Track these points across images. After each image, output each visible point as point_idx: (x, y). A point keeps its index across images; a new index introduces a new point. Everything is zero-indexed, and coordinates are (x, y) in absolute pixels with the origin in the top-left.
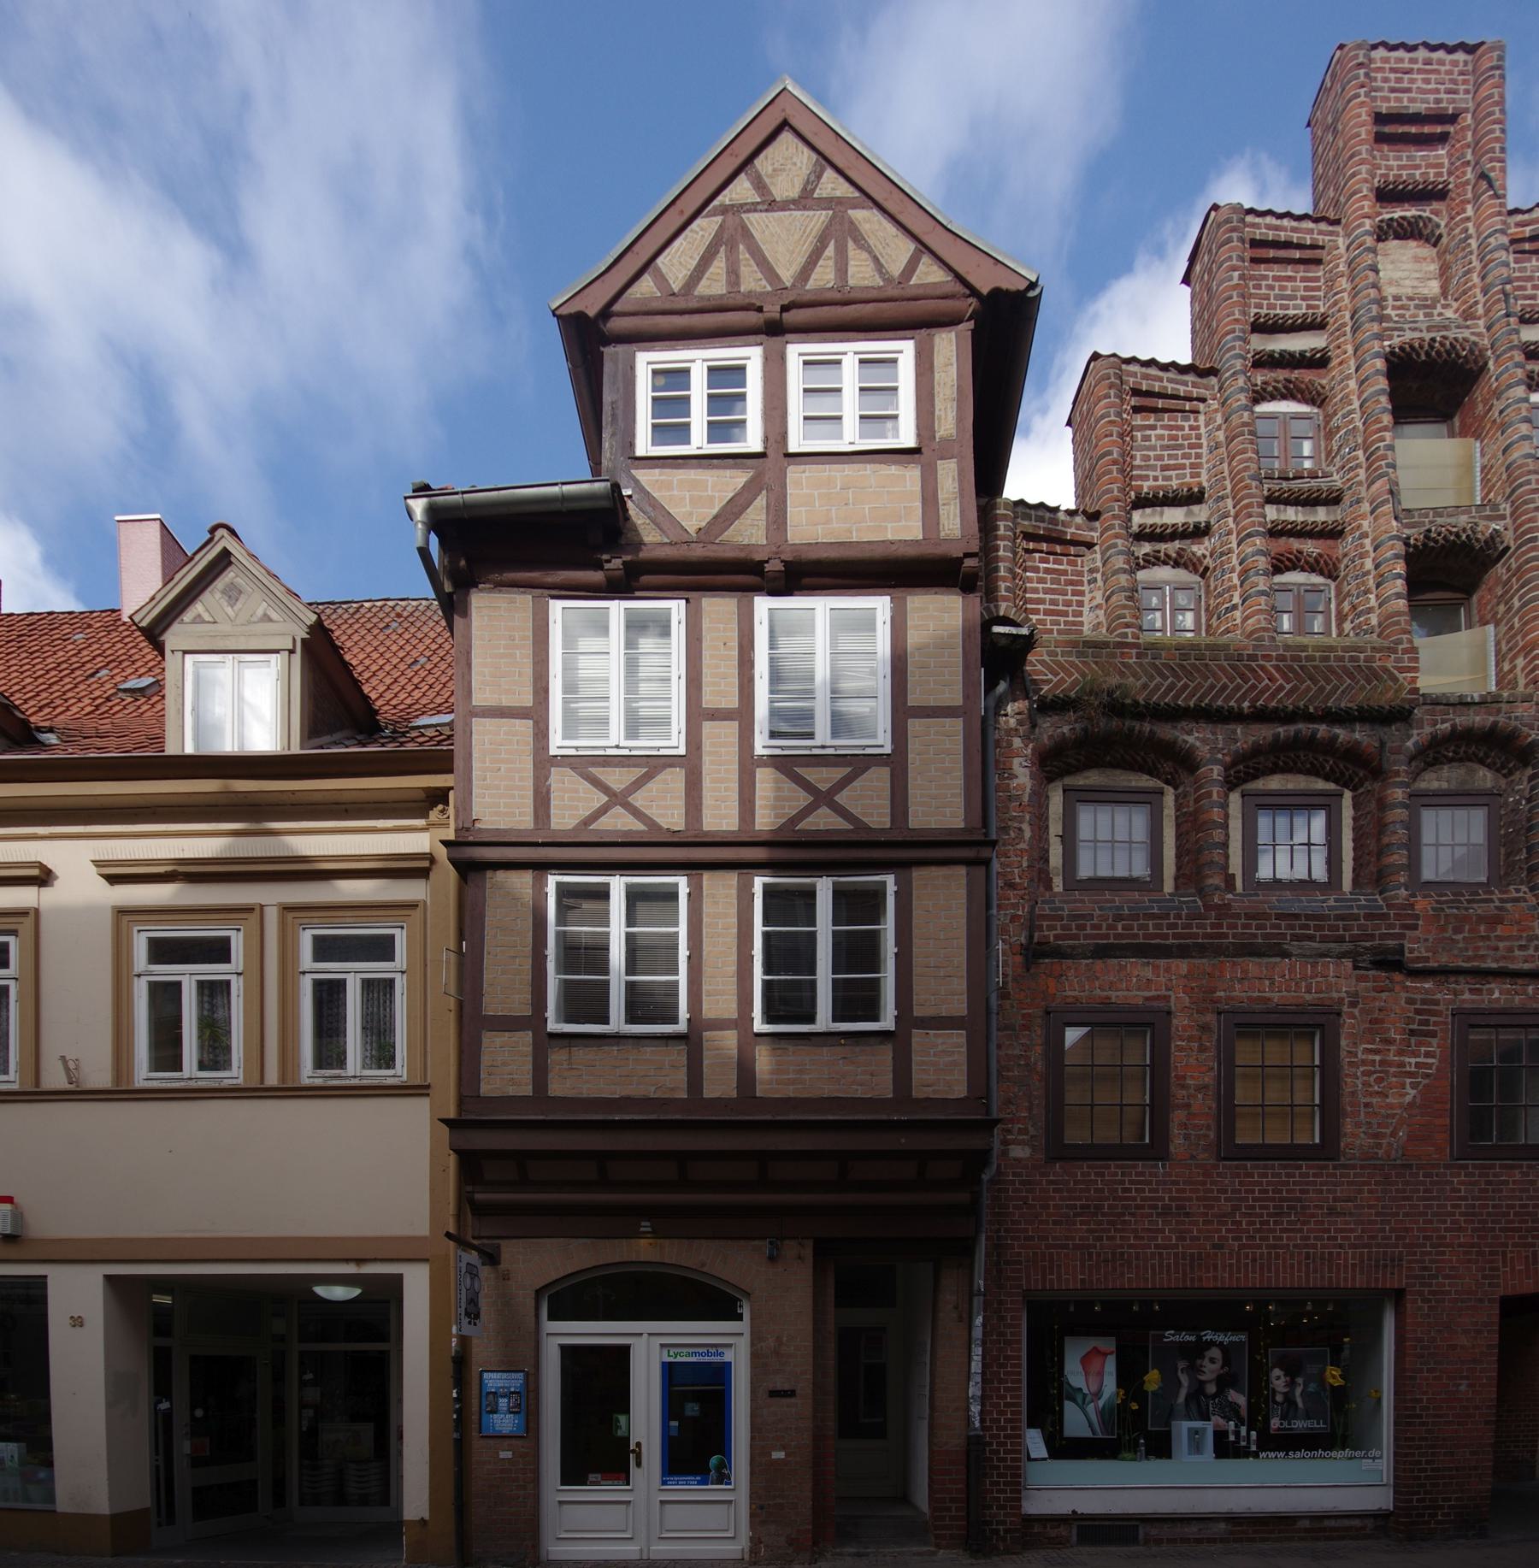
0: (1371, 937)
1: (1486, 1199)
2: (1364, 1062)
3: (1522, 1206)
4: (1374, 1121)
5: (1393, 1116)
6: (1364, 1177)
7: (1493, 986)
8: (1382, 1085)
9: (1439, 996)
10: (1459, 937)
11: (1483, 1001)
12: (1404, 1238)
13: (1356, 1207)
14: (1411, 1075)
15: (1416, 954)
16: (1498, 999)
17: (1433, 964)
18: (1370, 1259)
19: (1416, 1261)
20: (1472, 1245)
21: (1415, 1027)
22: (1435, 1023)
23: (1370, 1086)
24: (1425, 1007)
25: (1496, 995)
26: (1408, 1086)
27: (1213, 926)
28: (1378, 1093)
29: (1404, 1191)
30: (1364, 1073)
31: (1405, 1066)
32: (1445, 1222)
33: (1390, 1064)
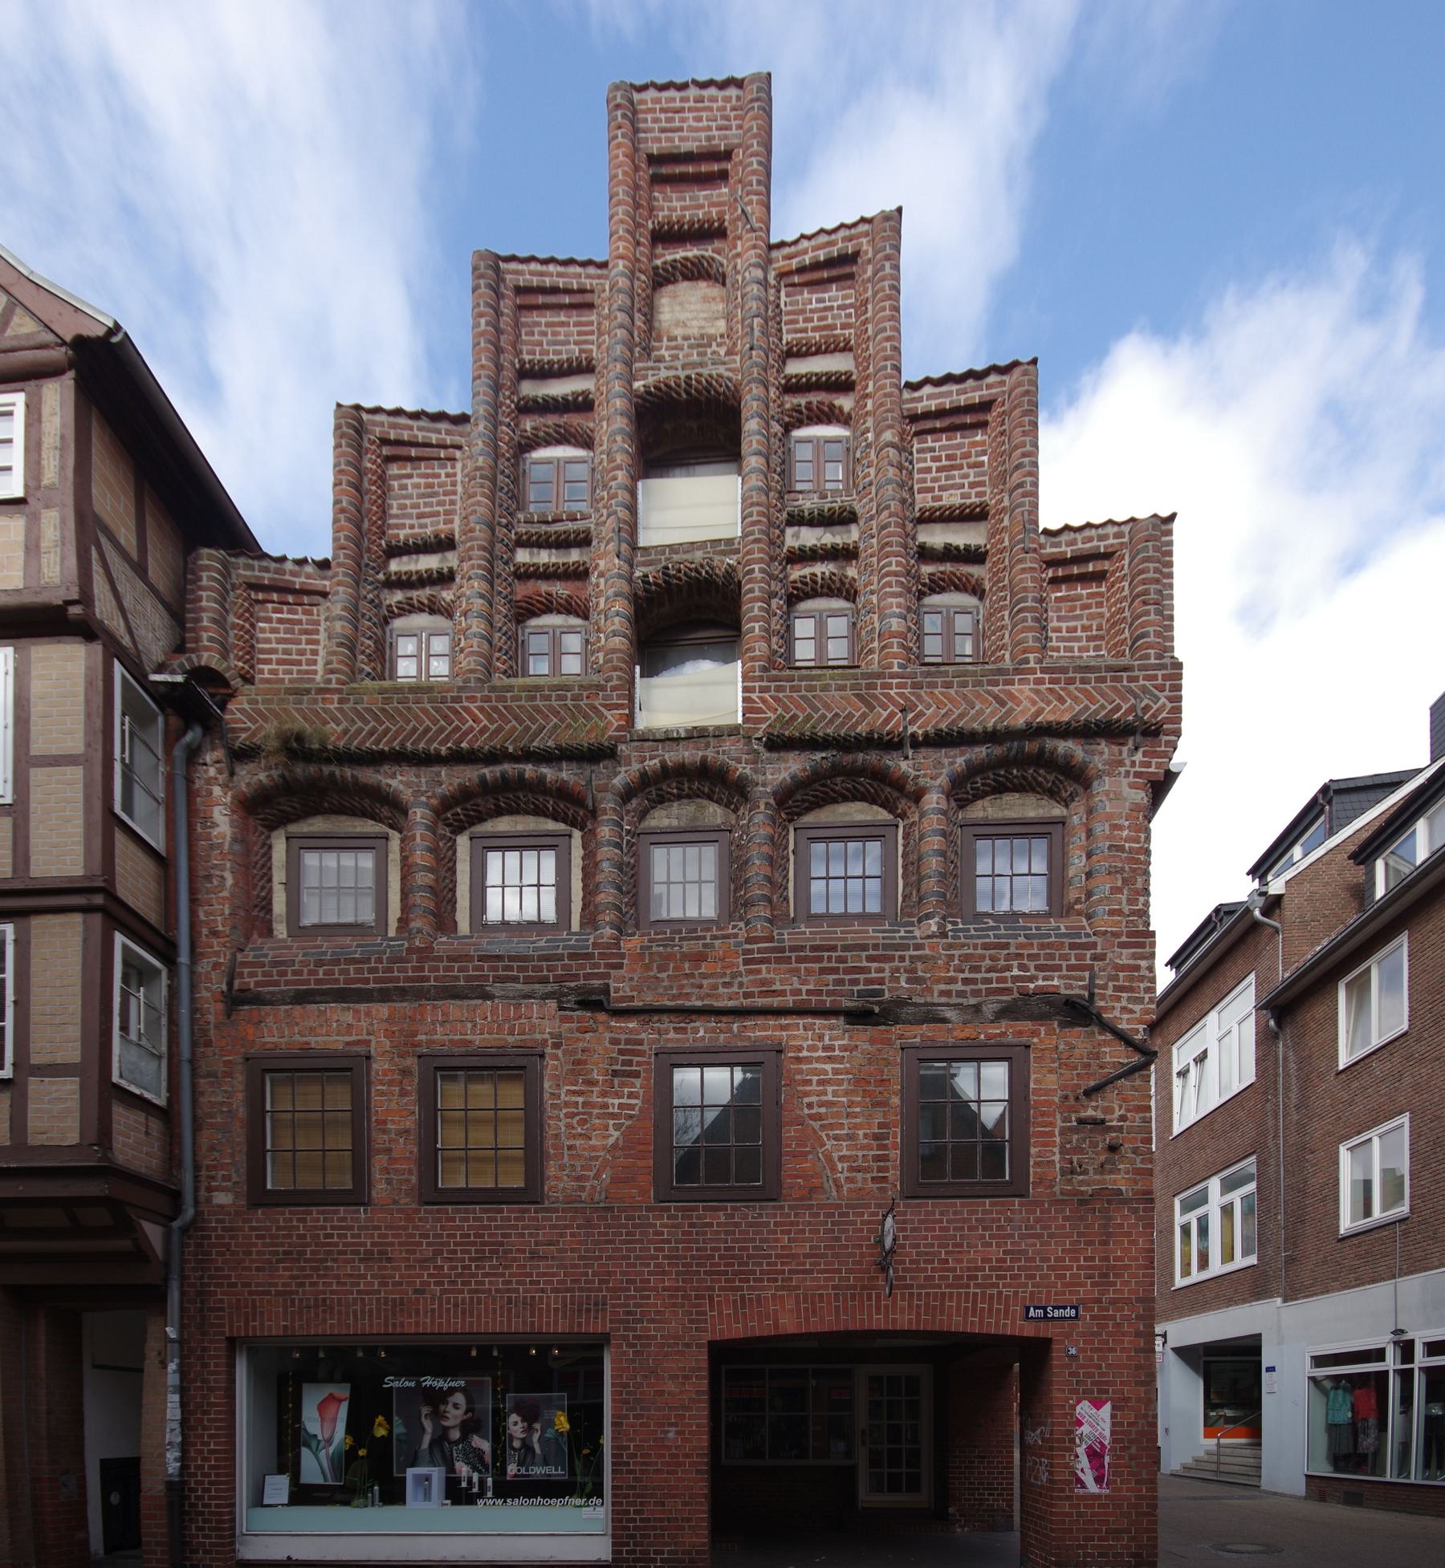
0: (576, 977)
1: (689, 1241)
3: (726, 1249)
4: (578, 1164)
5: (596, 1158)
7: (698, 1024)
9: (643, 1036)
12: (608, 1282)
13: (560, 1251)
15: (621, 993)
16: (703, 1038)
17: (637, 1003)
18: (572, 1303)
19: (619, 1306)
20: (677, 1289)
21: (618, 1067)
22: (639, 1064)
29: (607, 1234)
30: (567, 1116)
33: (592, 1105)
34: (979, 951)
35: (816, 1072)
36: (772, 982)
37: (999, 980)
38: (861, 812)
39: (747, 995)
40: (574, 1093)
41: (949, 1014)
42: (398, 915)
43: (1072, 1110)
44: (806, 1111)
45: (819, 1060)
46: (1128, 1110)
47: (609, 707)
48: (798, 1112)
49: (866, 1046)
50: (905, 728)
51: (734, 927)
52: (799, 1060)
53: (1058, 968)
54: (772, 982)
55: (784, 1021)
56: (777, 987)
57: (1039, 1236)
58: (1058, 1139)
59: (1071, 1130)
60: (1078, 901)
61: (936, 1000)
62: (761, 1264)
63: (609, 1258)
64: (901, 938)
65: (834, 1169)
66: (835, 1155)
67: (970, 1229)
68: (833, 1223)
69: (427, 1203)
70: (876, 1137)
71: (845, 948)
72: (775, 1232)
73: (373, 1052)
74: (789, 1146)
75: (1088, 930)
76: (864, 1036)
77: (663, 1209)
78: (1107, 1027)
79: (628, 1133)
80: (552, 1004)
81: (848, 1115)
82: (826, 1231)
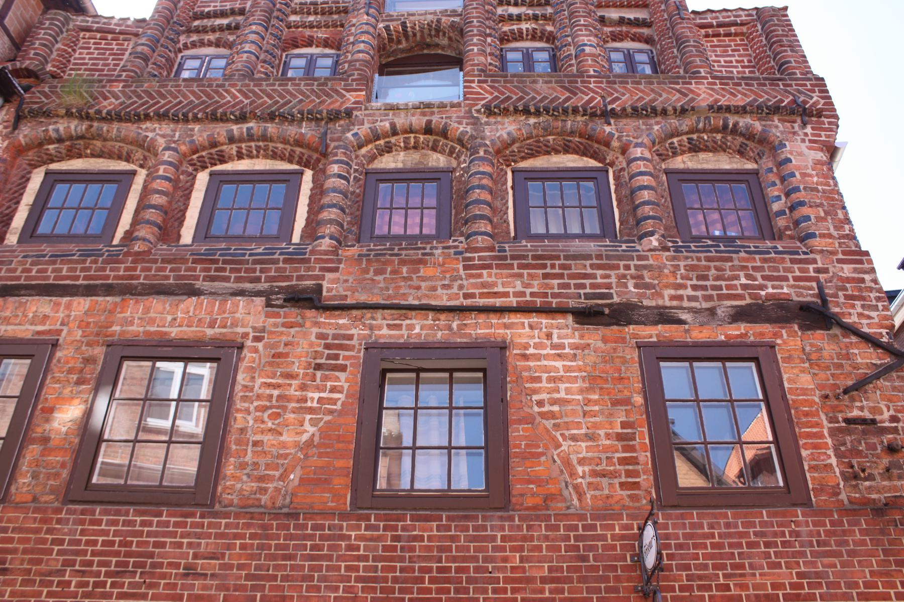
0: (289, 278)
2: (259, 397)
3: (440, 570)
5: (285, 456)
6: (237, 528)
7: (414, 321)
8: (276, 422)
9: (354, 331)
10: (380, 278)
11: (402, 336)
13: (223, 567)
14: (311, 410)
15: (334, 292)
16: (419, 335)
17: (349, 301)
21: (323, 361)
22: (345, 358)
23: (263, 422)
24: (336, 342)
25: (417, 330)
26: (307, 424)
27: (127, 269)
28: (270, 430)
29: (286, 547)
30: (257, 409)
31: (306, 401)
32: (336, 589)
33: (288, 399)
34: (704, 263)
35: (546, 369)
36: (495, 284)
37: (728, 287)
38: (574, 161)
39: (467, 296)
40: (269, 385)
41: (684, 316)
42: (127, 227)
43: (835, 409)
44: (536, 409)
45: (546, 357)
46: (896, 411)
47: (348, 91)
48: (529, 410)
49: (600, 344)
50: (605, 106)
51: (454, 241)
52: (525, 357)
53: (786, 279)
54: (495, 284)
55: (508, 319)
56: (500, 289)
57: (837, 554)
58: (829, 441)
59: (840, 430)
60: (787, 228)
61: (668, 303)
62: (485, 591)
63: (285, 578)
64: (623, 251)
65: (573, 474)
66: (574, 458)
67: (750, 545)
68: (577, 538)
69: (73, 502)
70: (620, 437)
71: (567, 258)
72: (503, 549)
73: (61, 341)
74: (519, 446)
75: (804, 250)
76: (595, 336)
77: (360, 518)
78: (851, 330)
79: (325, 432)
80: (260, 301)
81: (585, 414)
82: (568, 548)
